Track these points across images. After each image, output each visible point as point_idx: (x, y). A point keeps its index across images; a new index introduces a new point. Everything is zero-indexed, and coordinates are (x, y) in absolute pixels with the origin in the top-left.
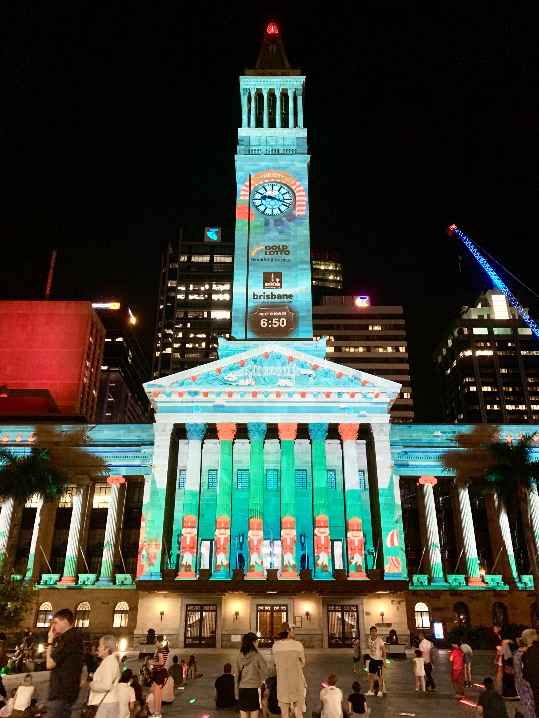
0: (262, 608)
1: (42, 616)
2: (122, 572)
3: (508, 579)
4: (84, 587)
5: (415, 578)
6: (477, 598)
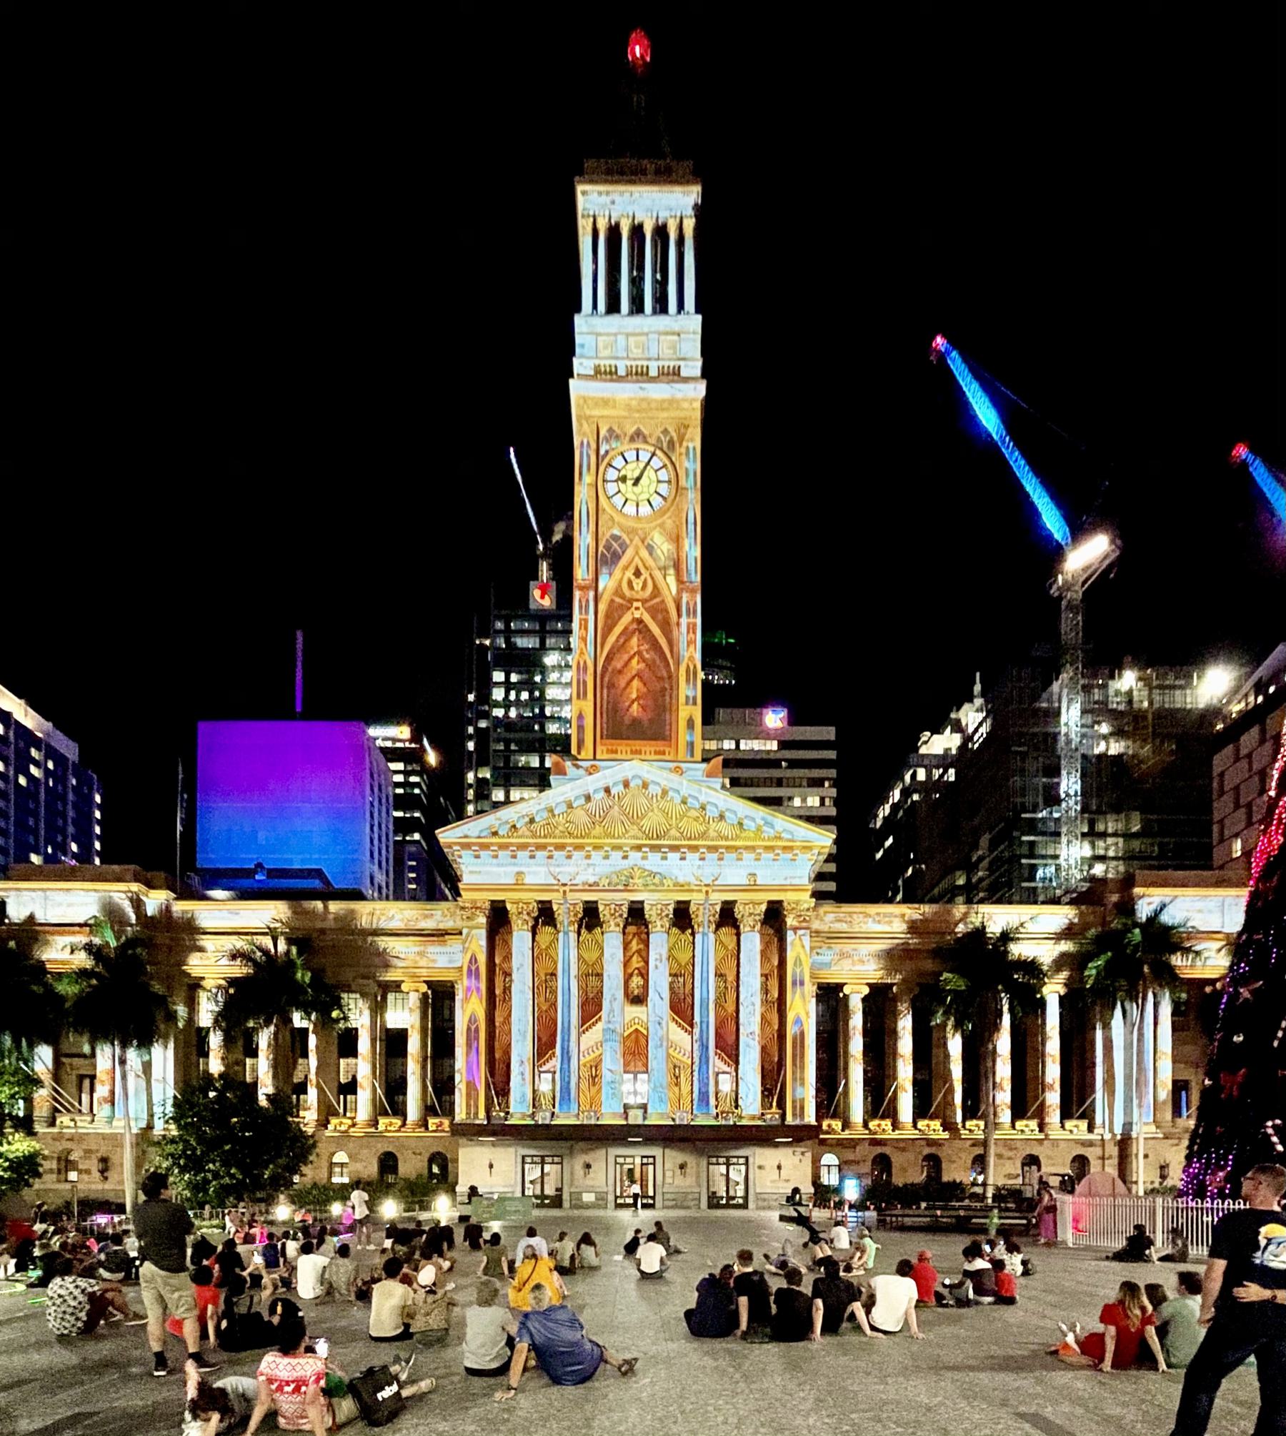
0: (621, 1160)
1: (337, 1170)
2: (436, 1114)
6: (903, 1150)
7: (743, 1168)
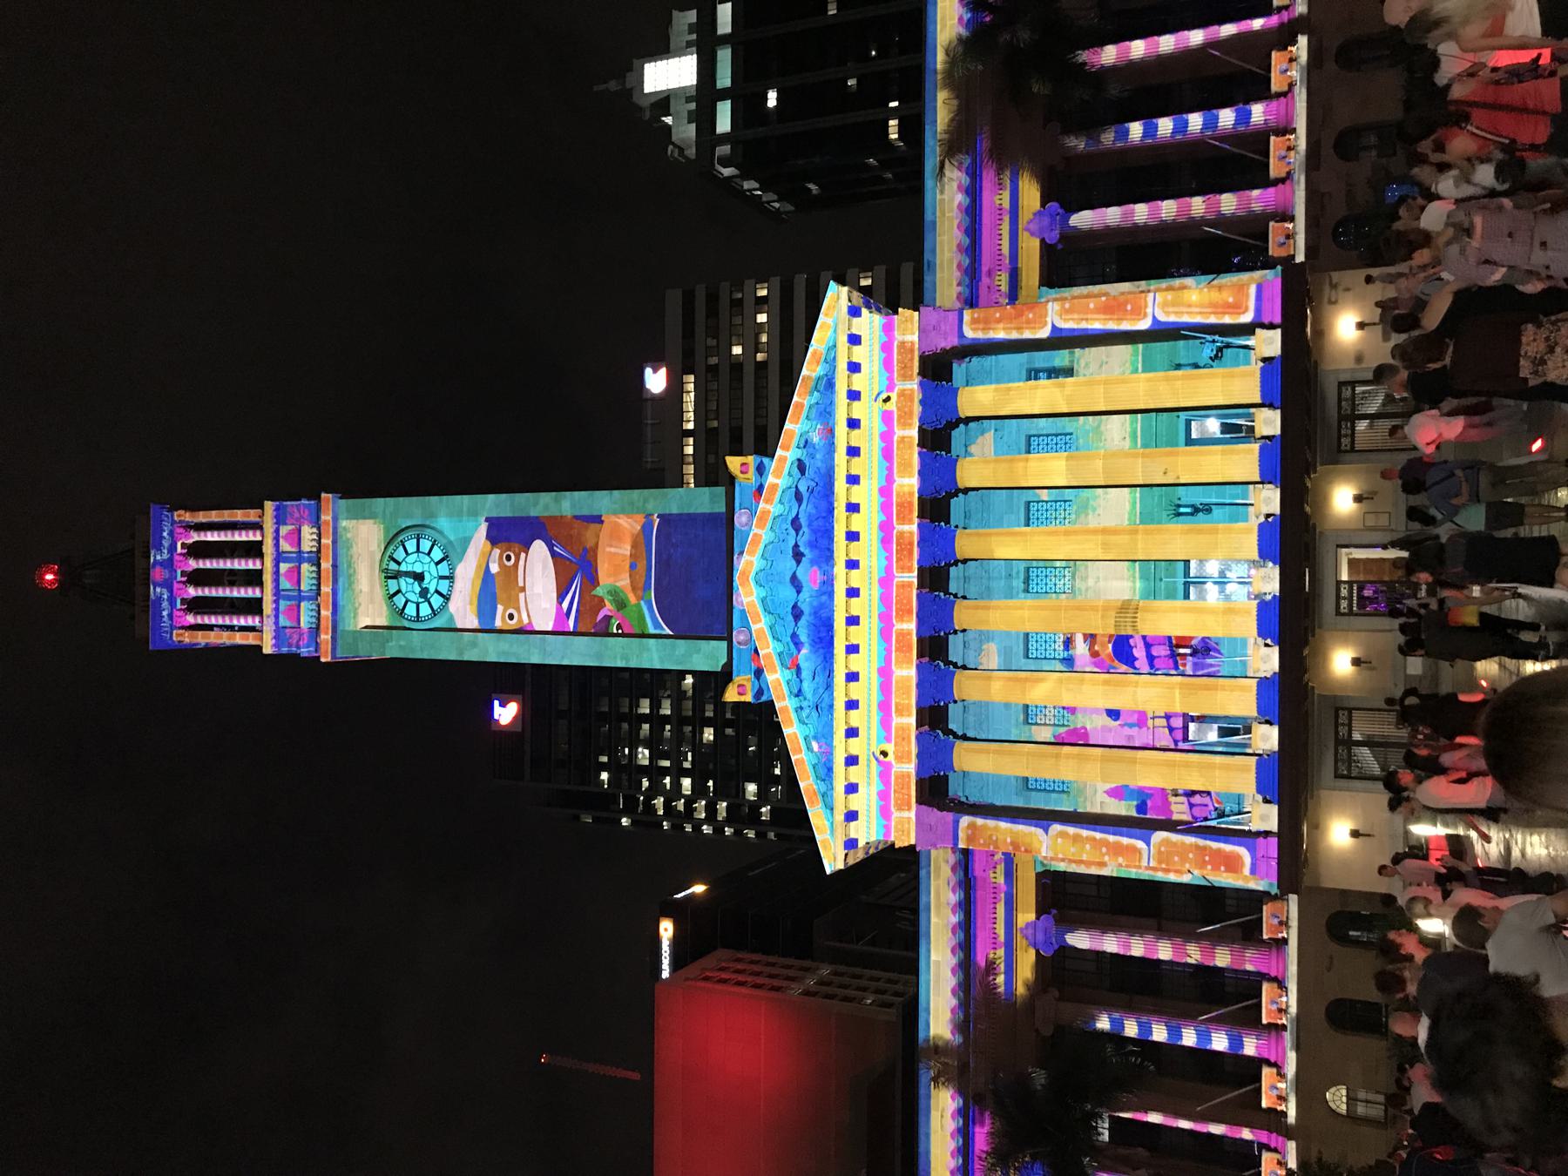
0: (1344, 604)
1: (1361, 1110)
3: (1284, 36)
4: (1293, 1010)
5: (1273, 251)
7: (1359, 389)
